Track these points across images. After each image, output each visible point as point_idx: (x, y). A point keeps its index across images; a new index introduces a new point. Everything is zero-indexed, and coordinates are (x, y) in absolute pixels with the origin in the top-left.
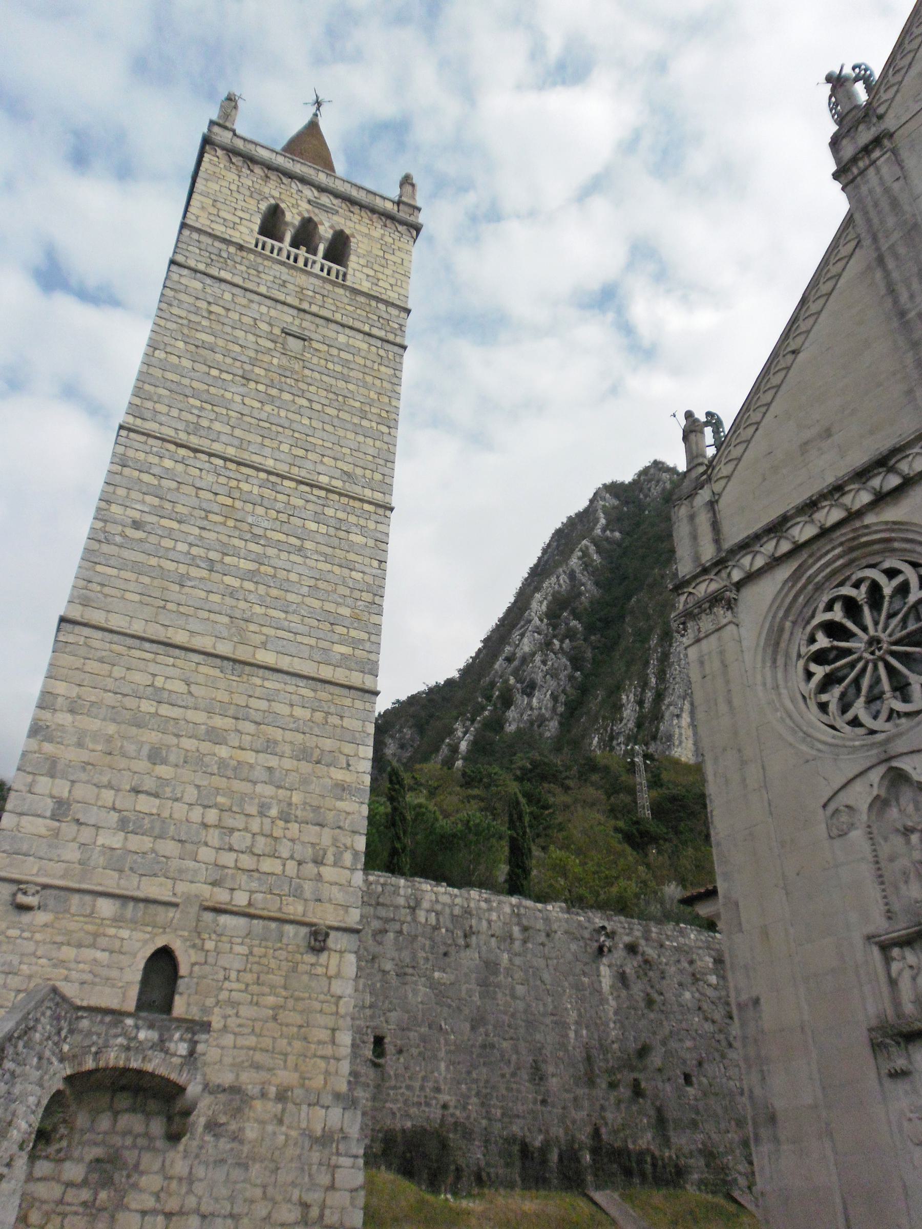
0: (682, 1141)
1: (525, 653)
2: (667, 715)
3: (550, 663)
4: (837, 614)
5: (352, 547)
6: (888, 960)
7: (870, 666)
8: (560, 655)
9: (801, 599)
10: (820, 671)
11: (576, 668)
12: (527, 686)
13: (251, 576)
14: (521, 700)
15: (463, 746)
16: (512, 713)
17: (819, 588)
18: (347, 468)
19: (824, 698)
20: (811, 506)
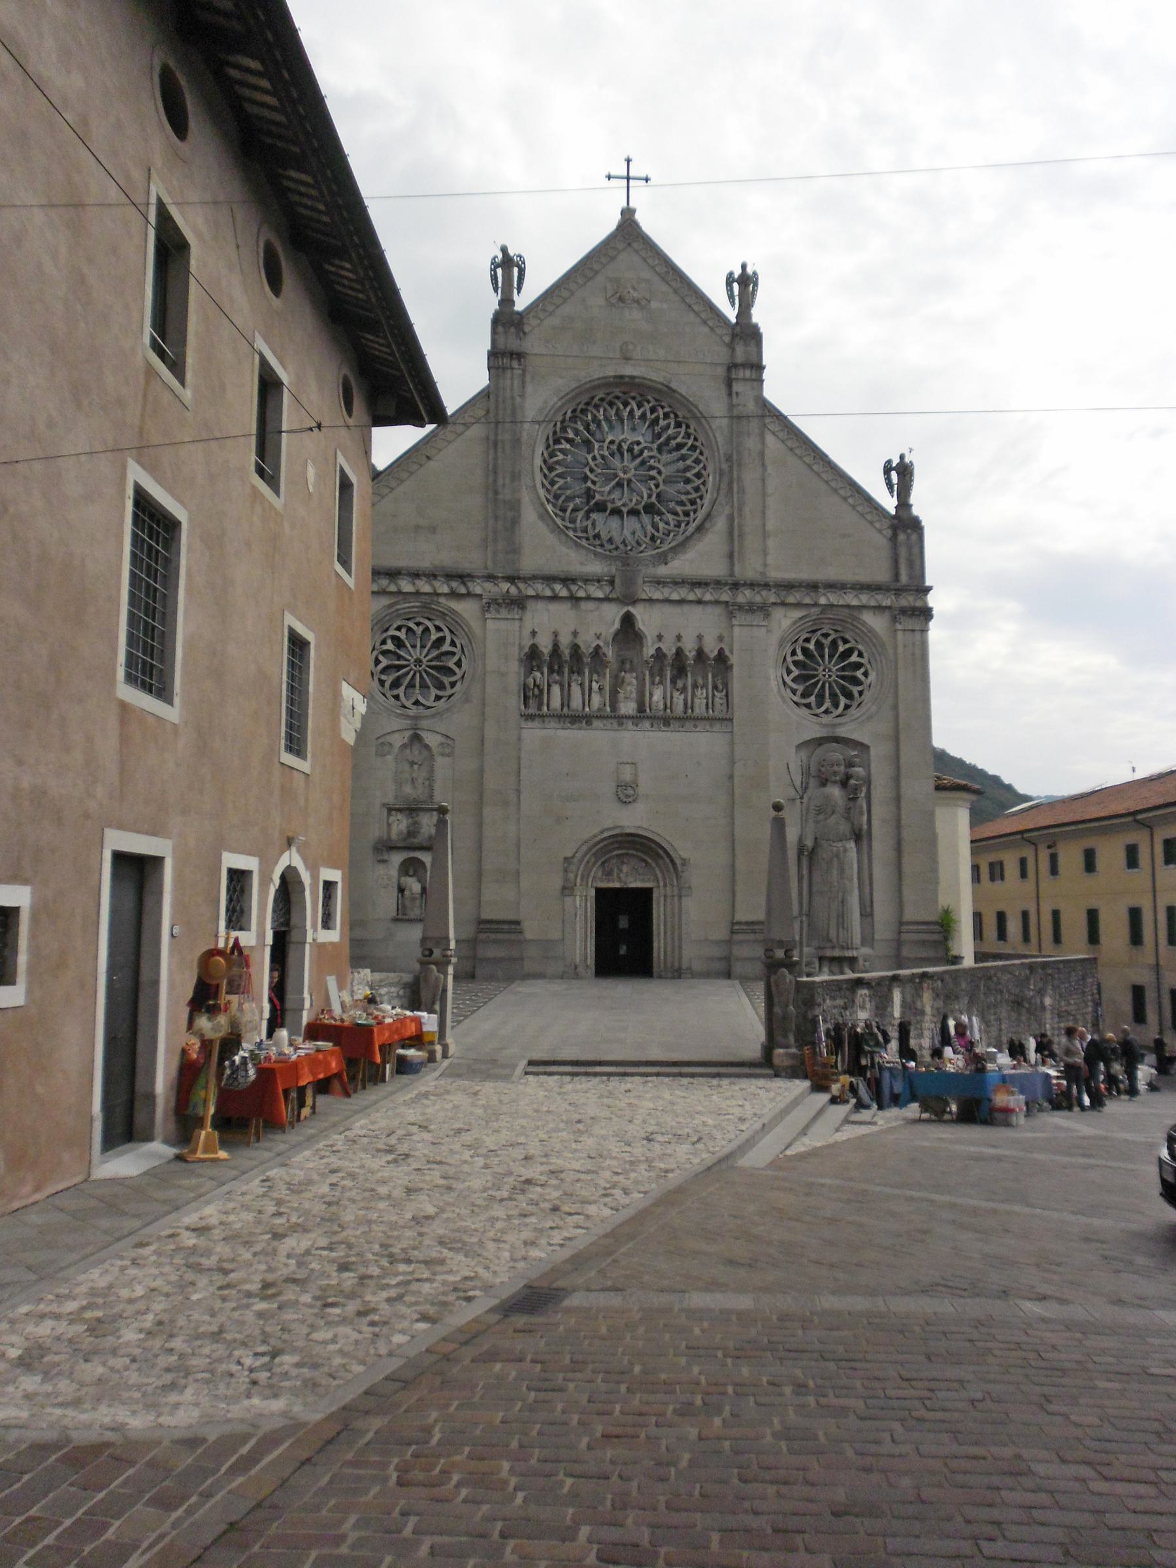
4: (402, 634)
6: (389, 814)
7: (412, 672)
9: (388, 618)
10: (385, 662)
17: (398, 616)
19: (383, 677)
20: (415, 575)
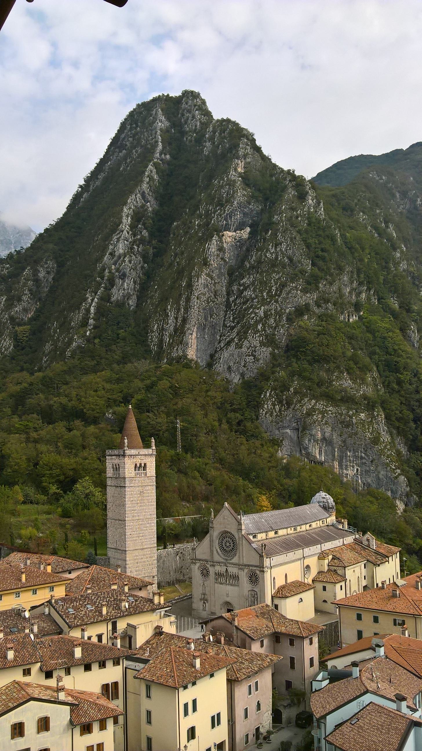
0: (185, 577)
1: (120, 254)
2: (187, 333)
3: (133, 262)
5: (153, 526)
8: (137, 256)
11: (145, 262)
12: (122, 275)
13: (142, 536)
14: (118, 282)
15: (92, 310)
16: (114, 290)
18: (150, 513)
